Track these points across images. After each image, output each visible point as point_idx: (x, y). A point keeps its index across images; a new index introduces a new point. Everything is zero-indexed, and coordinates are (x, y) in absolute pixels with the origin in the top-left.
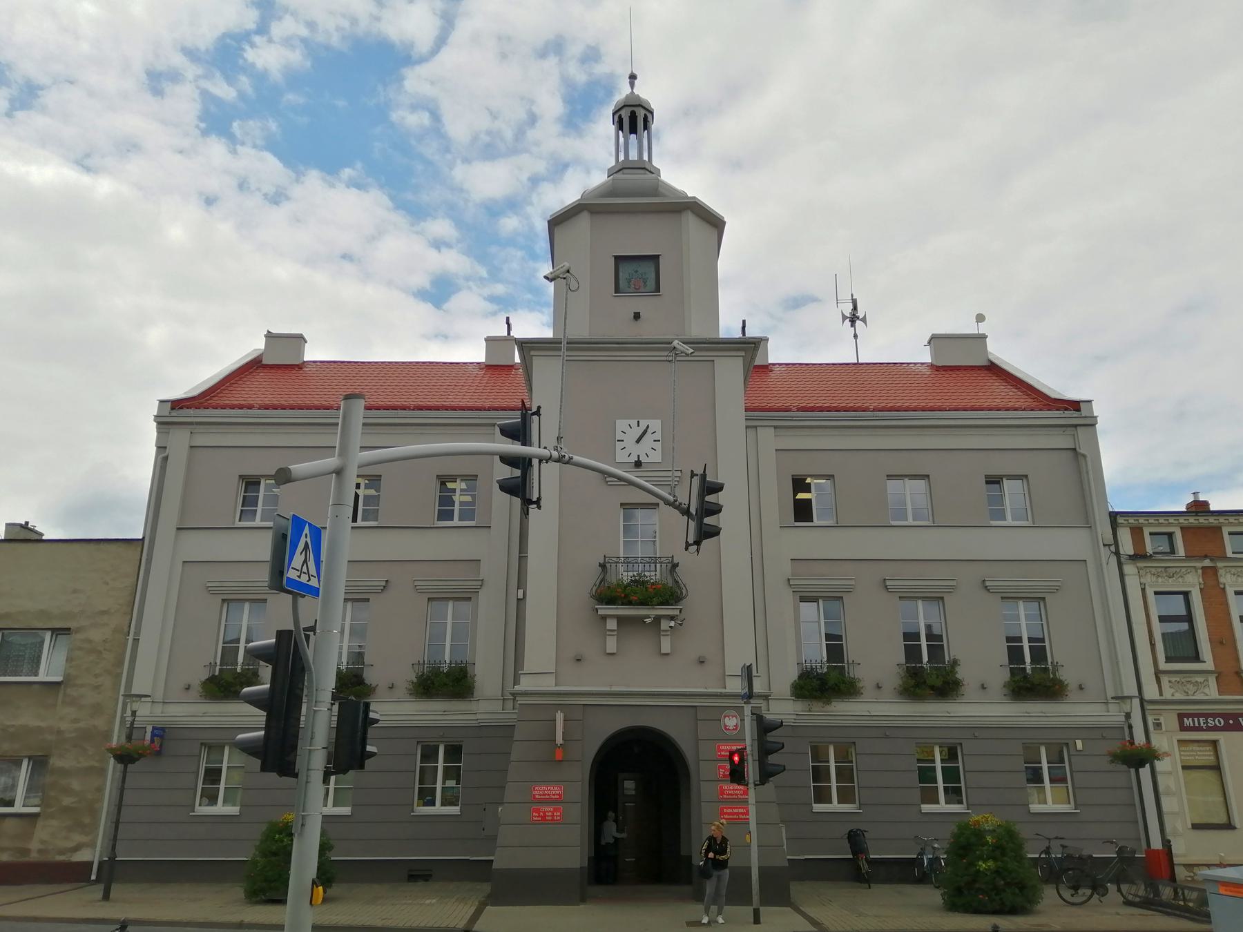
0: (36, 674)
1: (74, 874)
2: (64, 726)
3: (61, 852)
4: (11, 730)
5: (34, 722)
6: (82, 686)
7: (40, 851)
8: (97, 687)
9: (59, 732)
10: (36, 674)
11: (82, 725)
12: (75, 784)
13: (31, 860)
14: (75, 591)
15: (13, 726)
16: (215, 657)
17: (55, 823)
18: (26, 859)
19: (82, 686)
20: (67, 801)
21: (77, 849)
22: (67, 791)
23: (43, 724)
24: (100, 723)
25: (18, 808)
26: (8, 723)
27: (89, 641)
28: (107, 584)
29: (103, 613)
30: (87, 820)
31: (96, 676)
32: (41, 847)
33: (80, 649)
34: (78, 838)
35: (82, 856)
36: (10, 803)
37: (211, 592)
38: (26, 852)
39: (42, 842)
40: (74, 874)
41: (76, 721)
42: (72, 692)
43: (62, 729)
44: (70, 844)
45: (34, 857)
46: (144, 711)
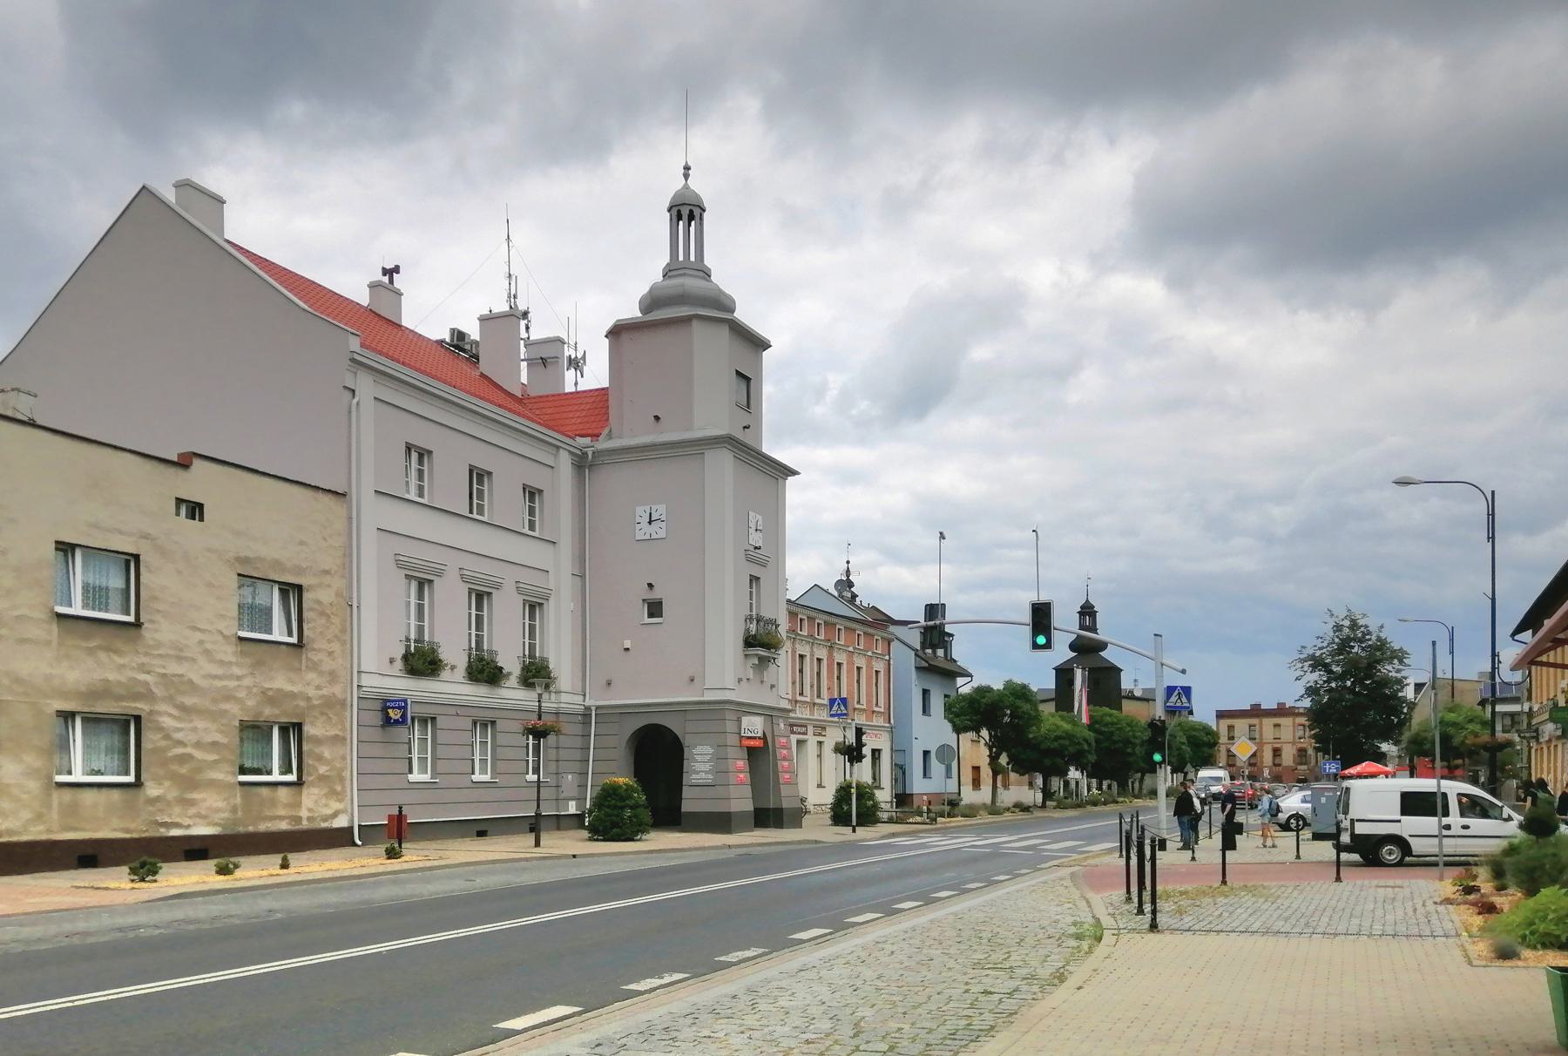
0: (270, 633)
1: (338, 839)
2: (311, 692)
3: (325, 819)
4: (270, 693)
5: (289, 688)
6: (319, 650)
7: (309, 819)
8: (330, 653)
9: (309, 699)
10: (270, 633)
11: (324, 692)
12: (327, 754)
13: (305, 827)
14: (302, 543)
15: (271, 689)
16: (470, 641)
17: (315, 791)
18: (301, 826)
19: (319, 650)
20: (323, 770)
21: (335, 815)
22: (320, 758)
23: (295, 689)
24: (337, 690)
25: (276, 777)
26: (267, 686)
27: (319, 602)
28: (325, 539)
29: (327, 572)
30: (339, 788)
31: (329, 641)
32: (310, 815)
33: (312, 609)
34: (335, 805)
35: (341, 822)
36: (269, 773)
37: (400, 565)
38: (298, 819)
39: (310, 810)
40: (338, 839)
41: (318, 688)
42: (315, 657)
43: (310, 695)
44: (329, 812)
45: (305, 825)
46: (367, 681)
